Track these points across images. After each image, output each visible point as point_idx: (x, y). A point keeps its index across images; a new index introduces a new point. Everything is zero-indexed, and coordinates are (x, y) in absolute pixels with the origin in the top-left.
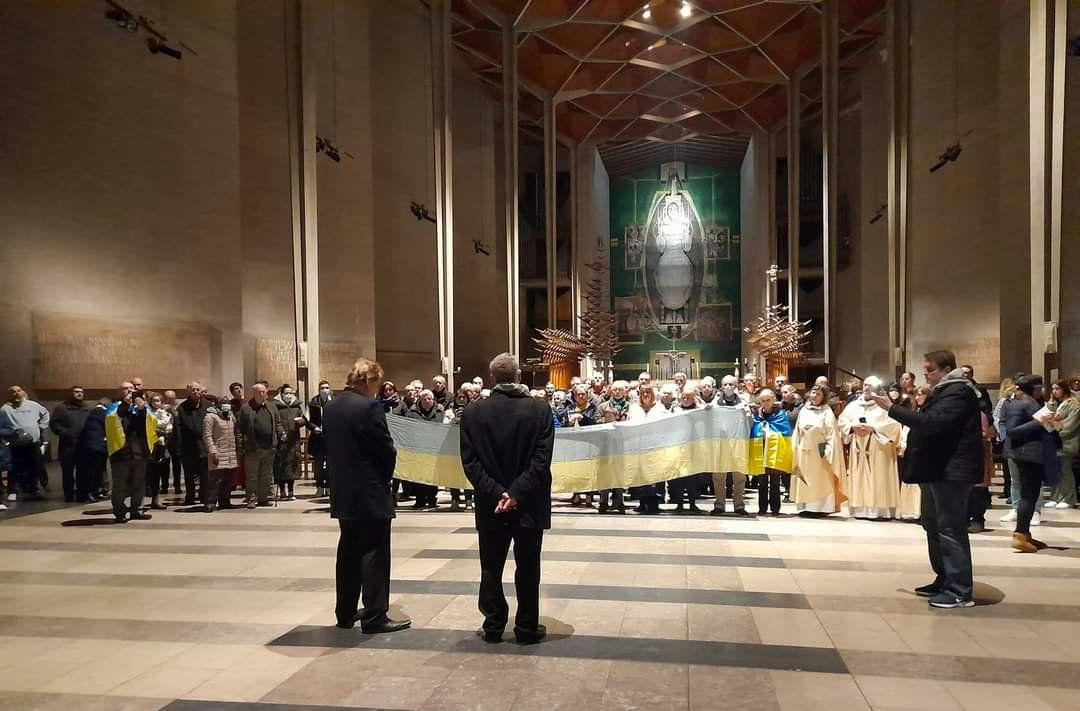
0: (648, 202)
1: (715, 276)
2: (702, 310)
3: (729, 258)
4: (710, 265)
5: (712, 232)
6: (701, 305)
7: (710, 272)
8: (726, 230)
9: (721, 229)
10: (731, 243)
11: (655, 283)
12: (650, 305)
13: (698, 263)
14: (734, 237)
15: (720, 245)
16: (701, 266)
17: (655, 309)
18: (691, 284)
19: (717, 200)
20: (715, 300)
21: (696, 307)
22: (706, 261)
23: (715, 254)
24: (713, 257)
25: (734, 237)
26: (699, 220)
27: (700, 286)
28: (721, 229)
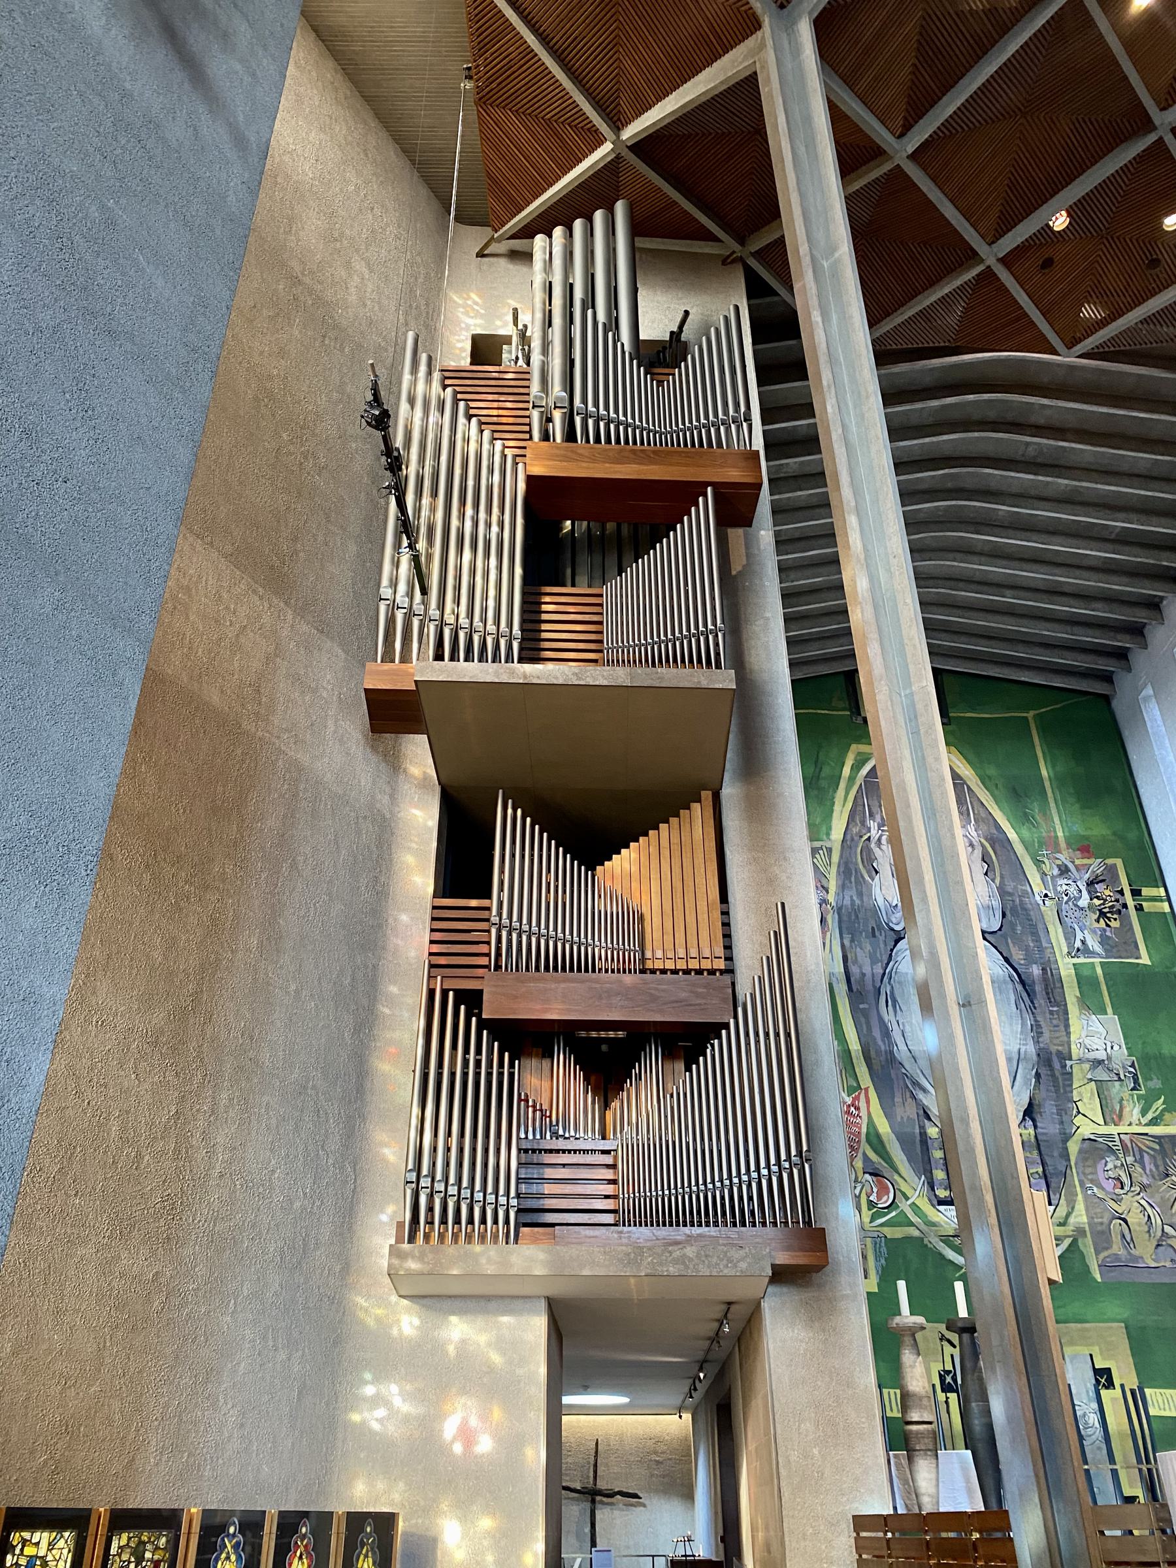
0: (826, 771)
1: (1111, 1018)
2: (1095, 1148)
3: (1145, 960)
4: (1086, 981)
5: (1064, 871)
6: (1085, 1128)
7: (1091, 1003)
8: (1112, 869)
9: (1096, 866)
10: (1139, 908)
11: (886, 1033)
12: (883, 1127)
13: (1036, 971)
14: (1145, 892)
15: (1102, 914)
16: (1052, 986)
17: (904, 1141)
18: (1030, 1049)
19: (1060, 781)
20: (1133, 1112)
21: (1066, 1137)
22: (1066, 967)
23: (1093, 944)
24: (1085, 950)
25: (1145, 892)
26: (1012, 835)
27: (1065, 1056)
28: (1096, 866)
